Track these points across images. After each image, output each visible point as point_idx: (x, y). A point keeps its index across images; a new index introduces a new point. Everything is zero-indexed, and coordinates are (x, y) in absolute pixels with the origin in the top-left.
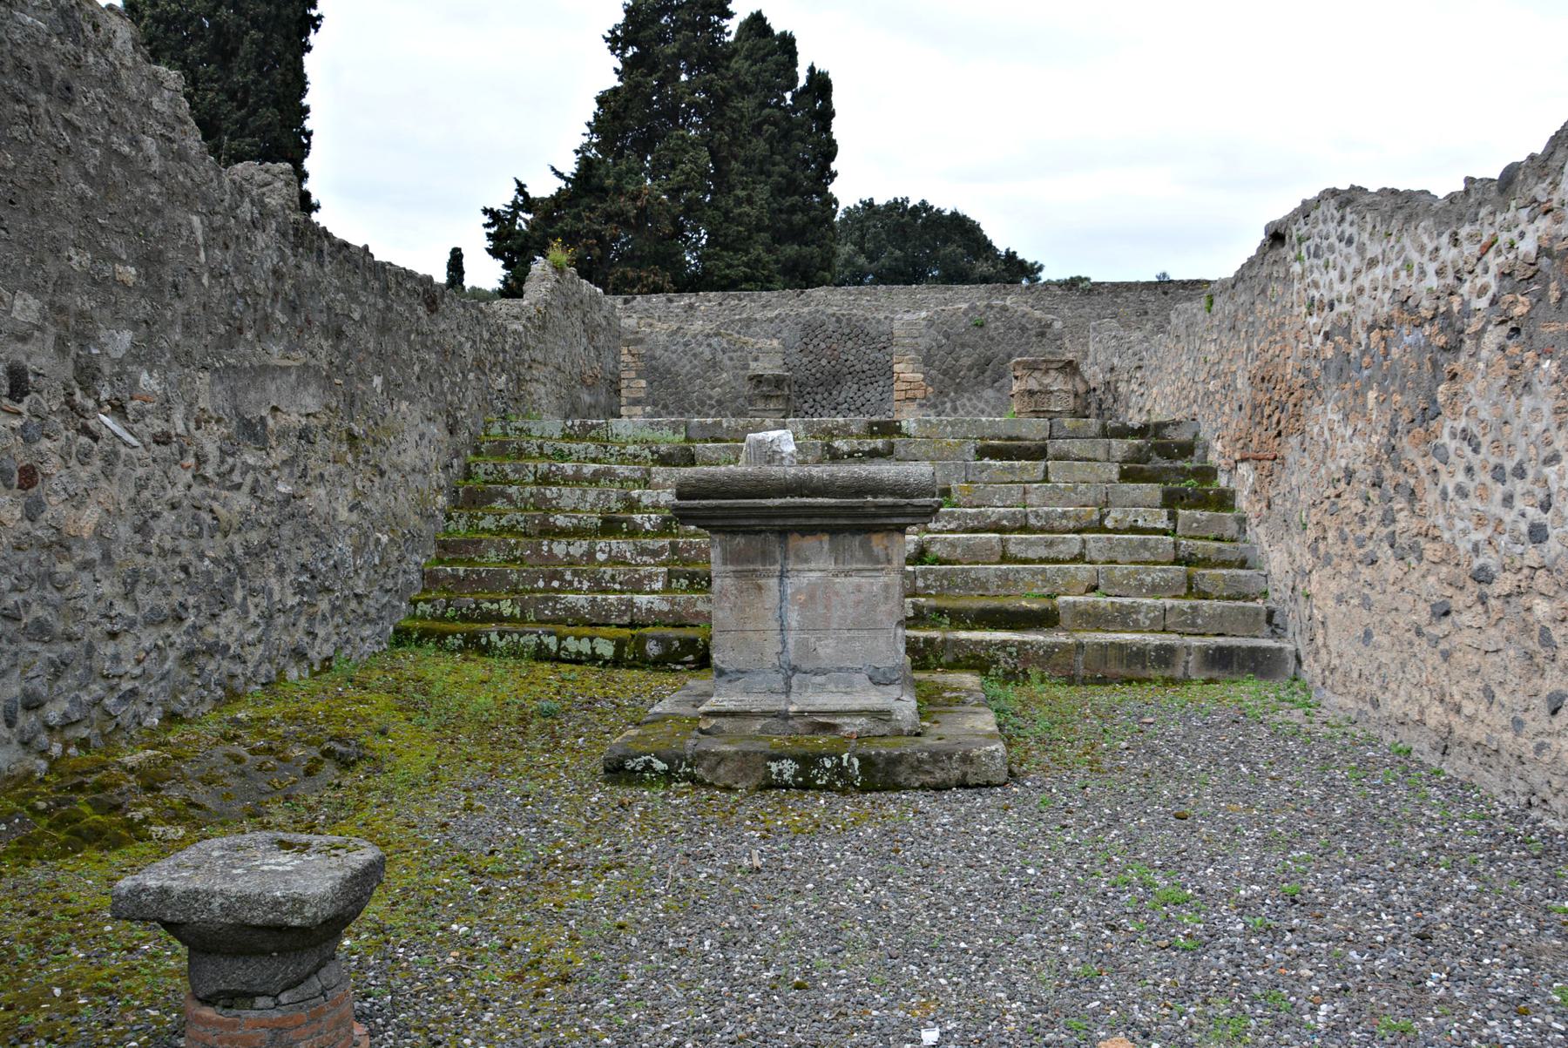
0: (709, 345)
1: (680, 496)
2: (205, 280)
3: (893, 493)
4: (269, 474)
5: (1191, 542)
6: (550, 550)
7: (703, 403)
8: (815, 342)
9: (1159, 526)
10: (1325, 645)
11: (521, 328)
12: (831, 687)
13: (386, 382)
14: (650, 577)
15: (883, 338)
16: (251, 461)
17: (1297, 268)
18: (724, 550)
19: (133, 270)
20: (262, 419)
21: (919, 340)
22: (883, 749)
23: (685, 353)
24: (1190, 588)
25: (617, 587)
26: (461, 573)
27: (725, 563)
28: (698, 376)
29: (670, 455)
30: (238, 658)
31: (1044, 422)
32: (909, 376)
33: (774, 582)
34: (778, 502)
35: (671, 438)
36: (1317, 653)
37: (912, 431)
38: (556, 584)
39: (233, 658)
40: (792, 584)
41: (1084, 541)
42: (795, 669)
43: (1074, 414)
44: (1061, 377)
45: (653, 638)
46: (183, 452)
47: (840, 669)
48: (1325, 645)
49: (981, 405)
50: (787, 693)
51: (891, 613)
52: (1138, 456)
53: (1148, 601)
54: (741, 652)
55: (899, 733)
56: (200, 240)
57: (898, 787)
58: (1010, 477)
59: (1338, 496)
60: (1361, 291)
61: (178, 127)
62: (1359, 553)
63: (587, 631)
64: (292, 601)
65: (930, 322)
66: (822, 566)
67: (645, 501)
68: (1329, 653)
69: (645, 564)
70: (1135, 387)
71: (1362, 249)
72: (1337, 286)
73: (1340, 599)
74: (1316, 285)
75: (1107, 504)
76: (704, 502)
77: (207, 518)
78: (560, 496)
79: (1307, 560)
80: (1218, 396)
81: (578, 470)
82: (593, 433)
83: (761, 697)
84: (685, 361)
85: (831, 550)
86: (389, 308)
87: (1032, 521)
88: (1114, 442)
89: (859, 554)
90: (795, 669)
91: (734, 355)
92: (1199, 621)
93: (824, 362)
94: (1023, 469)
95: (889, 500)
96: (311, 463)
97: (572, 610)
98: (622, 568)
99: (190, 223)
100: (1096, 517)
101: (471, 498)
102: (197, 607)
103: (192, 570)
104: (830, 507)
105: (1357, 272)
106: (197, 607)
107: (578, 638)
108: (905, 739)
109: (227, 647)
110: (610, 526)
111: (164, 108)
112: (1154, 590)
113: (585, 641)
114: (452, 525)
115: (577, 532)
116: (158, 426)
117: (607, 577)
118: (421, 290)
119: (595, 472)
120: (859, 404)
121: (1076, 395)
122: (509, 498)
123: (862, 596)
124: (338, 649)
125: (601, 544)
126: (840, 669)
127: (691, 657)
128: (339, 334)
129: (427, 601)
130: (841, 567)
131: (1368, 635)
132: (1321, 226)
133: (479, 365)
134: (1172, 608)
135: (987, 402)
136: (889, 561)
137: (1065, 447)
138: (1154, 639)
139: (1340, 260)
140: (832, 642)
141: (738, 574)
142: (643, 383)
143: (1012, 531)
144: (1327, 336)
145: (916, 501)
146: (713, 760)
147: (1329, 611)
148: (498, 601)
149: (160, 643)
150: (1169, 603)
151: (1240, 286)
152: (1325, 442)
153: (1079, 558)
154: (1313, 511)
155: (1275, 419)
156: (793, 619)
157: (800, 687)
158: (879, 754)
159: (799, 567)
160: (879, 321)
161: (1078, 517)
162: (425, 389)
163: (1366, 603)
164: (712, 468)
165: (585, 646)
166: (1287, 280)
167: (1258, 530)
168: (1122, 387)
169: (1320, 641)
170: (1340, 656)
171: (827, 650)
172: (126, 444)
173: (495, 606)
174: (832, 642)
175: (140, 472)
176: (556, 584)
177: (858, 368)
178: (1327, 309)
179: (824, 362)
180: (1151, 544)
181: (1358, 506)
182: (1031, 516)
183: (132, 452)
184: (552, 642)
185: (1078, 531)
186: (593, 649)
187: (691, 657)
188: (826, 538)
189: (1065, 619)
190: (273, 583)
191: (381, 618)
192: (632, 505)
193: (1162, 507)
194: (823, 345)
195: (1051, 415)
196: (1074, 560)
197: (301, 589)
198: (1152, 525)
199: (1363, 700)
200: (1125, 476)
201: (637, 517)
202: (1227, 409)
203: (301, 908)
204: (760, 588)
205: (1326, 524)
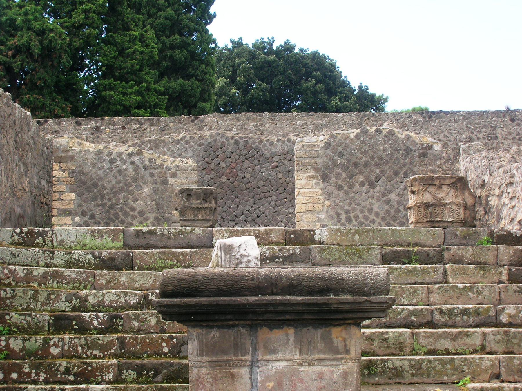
0: (133, 163)
1: (164, 294)
3: (353, 292)
6: (8, 345)
7: (126, 214)
8: (216, 161)
14: (103, 369)
15: (276, 158)
18: (200, 342)
21: (318, 160)
23: (110, 169)
25: (71, 378)
28: (122, 190)
29: (112, 259)
31: (438, 230)
32: (308, 191)
33: (245, 371)
34: (252, 299)
35: (110, 244)
37: (324, 239)
38: (14, 376)
41: (485, 335)
43: (464, 223)
44: (452, 192)
49: (372, 217)
58: (413, 279)
65: (328, 145)
66: (288, 357)
67: (92, 300)
69: (95, 357)
70: (507, 201)
75: (500, 302)
76: (185, 300)
78: (13, 297)
81: (29, 274)
82: (40, 240)
84: (111, 176)
85: (296, 342)
87: (437, 317)
88: (501, 248)
89: (320, 345)
91: (154, 171)
93: (224, 179)
95: (349, 297)
98: (74, 361)
100: (492, 313)
104: (298, 304)
110: (61, 323)
115: (33, 330)
117: (62, 369)
119: (45, 276)
121: (466, 207)
123: (324, 383)
125: (55, 338)
130: (305, 356)
135: (377, 214)
136: (347, 352)
137: (459, 252)
141: (213, 364)
142: (73, 196)
143: (420, 326)
145: (373, 298)
153: (482, 349)
159: (268, 357)
160: (272, 144)
161: (477, 312)
164: (191, 270)
168: (493, 201)
176: (14, 376)
177: (254, 184)
179: (224, 179)
182: (436, 313)
185: (477, 326)
188: (291, 331)
194: (223, 164)
195: (444, 225)
196: (475, 352)
201: (86, 315)
204: (233, 376)
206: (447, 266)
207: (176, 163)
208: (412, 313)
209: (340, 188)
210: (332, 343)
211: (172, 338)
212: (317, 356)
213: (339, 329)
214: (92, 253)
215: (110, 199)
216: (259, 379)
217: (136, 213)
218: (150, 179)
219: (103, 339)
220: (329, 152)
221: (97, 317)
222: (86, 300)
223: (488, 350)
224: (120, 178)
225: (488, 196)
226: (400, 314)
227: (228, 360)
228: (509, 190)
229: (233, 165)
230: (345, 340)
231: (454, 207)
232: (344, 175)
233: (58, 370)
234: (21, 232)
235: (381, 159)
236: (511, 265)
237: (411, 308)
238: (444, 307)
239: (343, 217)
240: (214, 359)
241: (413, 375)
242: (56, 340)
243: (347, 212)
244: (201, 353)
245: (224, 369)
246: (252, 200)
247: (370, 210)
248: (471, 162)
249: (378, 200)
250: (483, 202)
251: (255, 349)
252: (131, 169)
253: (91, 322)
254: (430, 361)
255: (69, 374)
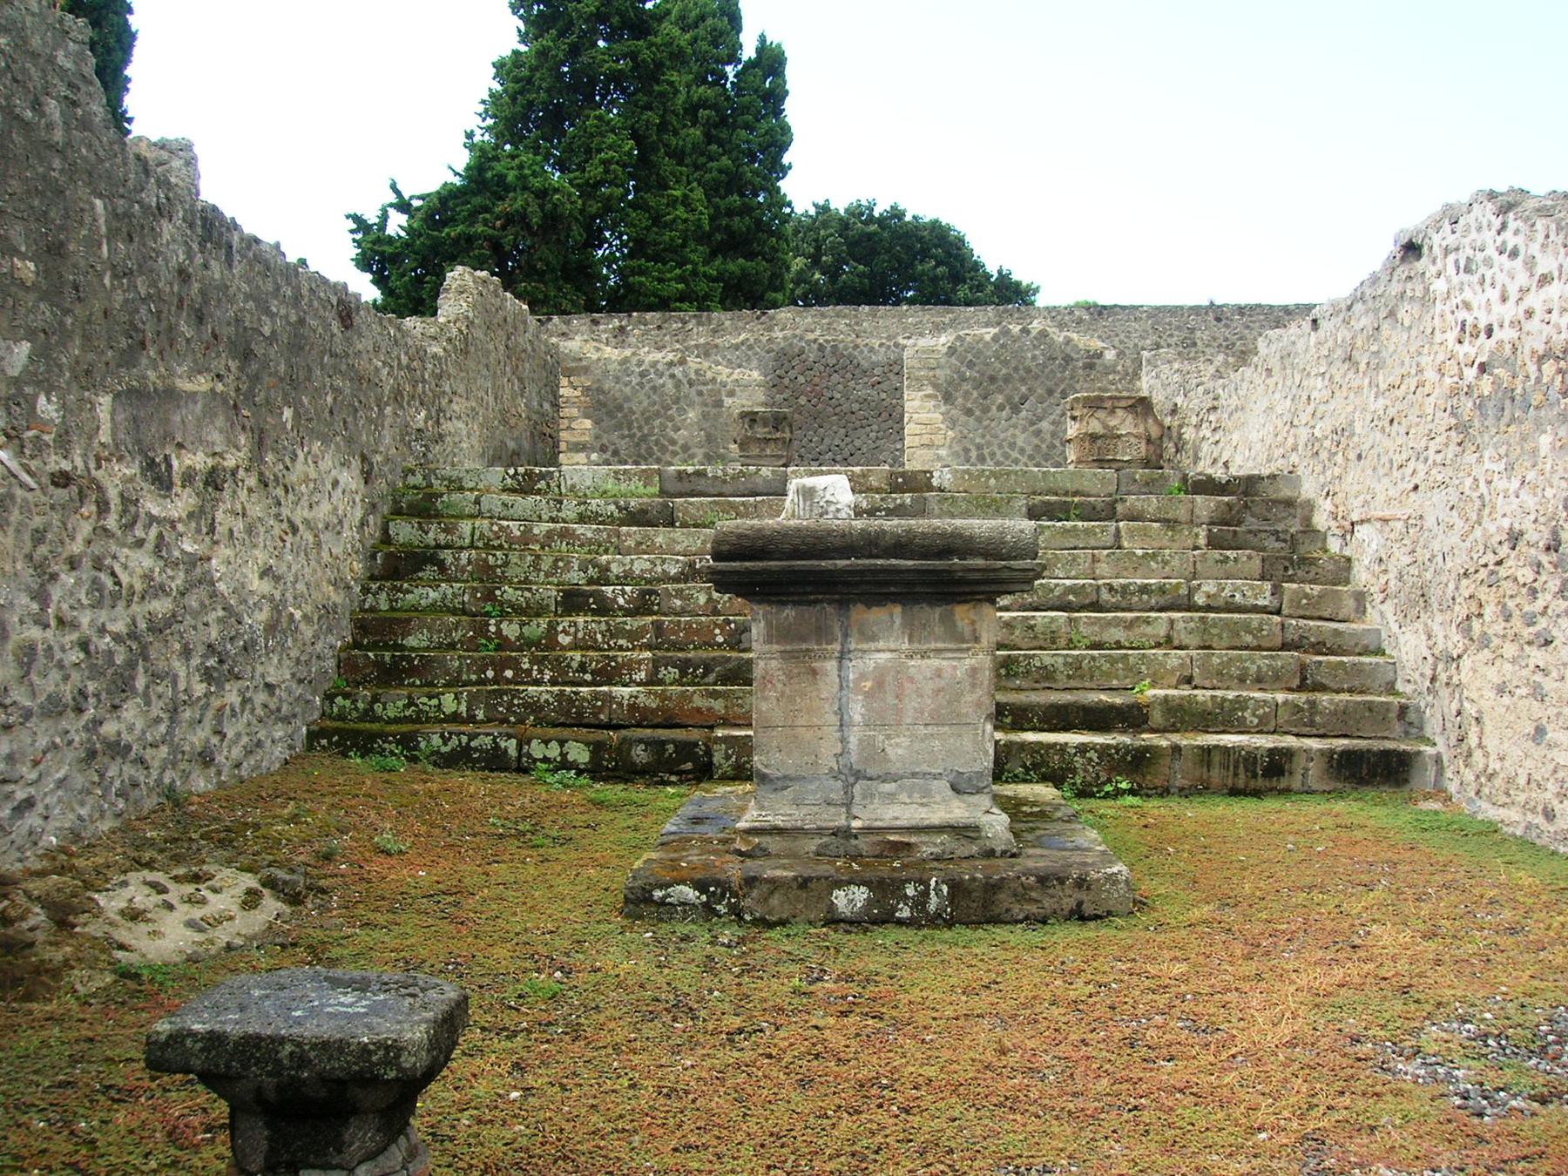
0: (672, 376)
1: (717, 556)
2: (107, 281)
3: (986, 555)
4: (174, 527)
5: (1302, 622)
6: (499, 631)
7: (663, 449)
8: (792, 374)
9: (1261, 602)
10: (1480, 746)
11: (441, 353)
12: (904, 797)
13: (297, 416)
14: (631, 666)
16: (155, 511)
17: (1439, 286)
18: (769, 625)
19: (31, 266)
20: (167, 459)
21: (938, 372)
22: (973, 872)
23: (641, 385)
24: (1304, 679)
25: (588, 677)
26: (387, 659)
27: (770, 642)
28: (657, 415)
29: (643, 512)
30: (141, 761)
31: (1110, 473)
32: (924, 416)
33: (831, 666)
34: (841, 563)
35: (641, 490)
36: (1470, 755)
37: (946, 484)
38: (509, 673)
39: (133, 762)
40: (854, 668)
41: (1172, 622)
42: (858, 775)
43: (1146, 463)
45: (640, 741)
46: (82, 497)
47: (914, 775)
48: (1480, 746)
49: (1015, 454)
50: (848, 805)
51: (979, 705)
52: (1227, 519)
53: (1258, 695)
54: (789, 754)
55: (990, 854)
56: (104, 229)
57: (996, 920)
59: (1499, 563)
60: (1529, 314)
61: (83, 88)
62: (1527, 632)
63: (552, 731)
64: (199, 689)
65: (952, 351)
66: (893, 646)
67: (615, 569)
68: (1486, 755)
69: (621, 648)
70: (1208, 434)
71: (1530, 264)
72: (1497, 307)
73: (1501, 690)
74: (1467, 306)
75: (1195, 576)
76: (748, 564)
77: (108, 582)
78: (506, 564)
79: (1454, 641)
80: (1327, 443)
81: (528, 530)
82: (542, 485)
83: (815, 809)
86: (301, 322)
87: (1105, 596)
88: (1199, 499)
89: (939, 630)
90: (858, 775)
92: (1318, 719)
93: (803, 400)
94: (1086, 531)
96: (219, 516)
97: (534, 707)
99: (93, 207)
100: (1183, 591)
101: (396, 565)
102: (97, 696)
103: (92, 648)
104: (909, 570)
105: (1524, 291)
106: (97, 696)
107: (546, 742)
108: (1001, 862)
109: (128, 748)
110: (573, 601)
111: (68, 65)
112: (1260, 681)
113: (554, 744)
114: (370, 599)
116: (56, 463)
117: (575, 665)
118: (334, 301)
119: (549, 534)
120: (846, 453)
121: (1149, 441)
122: (441, 566)
123: (943, 683)
124: (249, 752)
125: (565, 622)
126: (914, 775)
127: (689, 766)
128: (246, 355)
129: (346, 696)
130: (916, 646)
131: (1540, 731)
132: (1474, 235)
133: (397, 396)
134: (1286, 703)
135: (1022, 451)
136: (977, 639)
137: (1139, 505)
138: (1265, 742)
139: (1501, 278)
140: (904, 741)
141: (787, 656)
142: (588, 423)
144: (1483, 368)
146: (765, 888)
147: (1485, 705)
148: (437, 696)
149: (58, 740)
150: (1280, 697)
151: (1358, 307)
152: (1481, 497)
153: (1168, 642)
154: (1465, 582)
155: (1409, 471)
156: (857, 711)
157: (864, 798)
158: (974, 879)
159: (865, 646)
160: (872, 350)
161: (1162, 590)
162: (339, 426)
163: (1538, 694)
165: (554, 751)
166: (1427, 300)
167: (1383, 607)
168: (1189, 434)
169: (1473, 740)
170: (1502, 759)
171: (898, 750)
172: (22, 485)
173: (434, 702)
174: (904, 741)
175: (38, 521)
176: (509, 673)
177: (845, 407)
178: (1483, 336)
179: (803, 400)
180: (1255, 624)
181: (1526, 575)
183: (29, 496)
184: (511, 746)
185: (1161, 610)
186: (563, 755)
187: (689, 766)
188: (898, 610)
189: (1157, 717)
190: (179, 667)
191: (295, 716)
192: (603, 578)
193: (1262, 578)
194: (801, 379)
195: (1118, 465)
196: (1158, 645)
197: (207, 675)
198: (1252, 601)
199: (1533, 810)
200: (1214, 543)
202: (1339, 458)
203: (398, 1057)
204: (814, 672)
205: (1483, 598)
206: (1121, 524)
207: (735, 376)
208: (1071, 590)
209: (969, 412)
210: (955, 626)
211: (729, 622)
212: (933, 646)
213: (966, 607)
214: (616, 503)
215: (640, 428)
216: (851, 677)
217: (677, 448)
218: (697, 399)
219: (632, 623)
220: (953, 360)
221: (624, 593)
222: (608, 570)
223: (1176, 643)
224: (655, 397)
225: (1181, 426)
226: (1052, 591)
227: (808, 650)
228: (1212, 418)
229: (816, 380)
230: (973, 623)
231: (1132, 440)
232: (975, 394)
233: (569, 666)
234: (516, 473)
235: (1028, 371)
236: (1212, 523)
237: (1068, 582)
238: (1116, 582)
239: (974, 454)
240: (788, 648)
241: (1069, 677)
242: (566, 624)
243: (979, 447)
244: (769, 640)
245: (802, 663)
246: (843, 431)
247: (1012, 445)
248: (1157, 377)
249: (1024, 430)
250: (1175, 435)
251: (846, 635)
252: (670, 384)
253: (614, 600)
254: (1093, 658)
255: (585, 672)
